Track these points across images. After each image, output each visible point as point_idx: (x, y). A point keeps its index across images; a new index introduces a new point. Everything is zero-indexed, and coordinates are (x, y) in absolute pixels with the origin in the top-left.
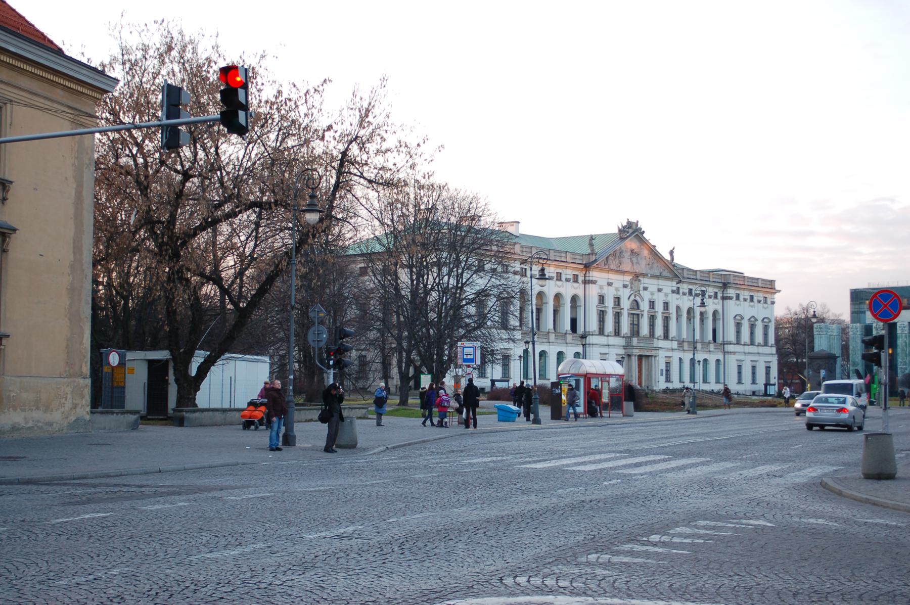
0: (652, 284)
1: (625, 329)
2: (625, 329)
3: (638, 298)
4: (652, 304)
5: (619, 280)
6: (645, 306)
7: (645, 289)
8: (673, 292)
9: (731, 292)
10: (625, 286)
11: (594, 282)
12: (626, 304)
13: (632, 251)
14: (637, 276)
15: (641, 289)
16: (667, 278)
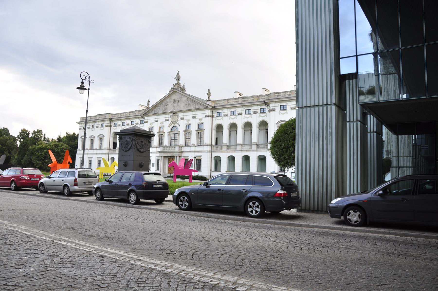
0: (188, 116)
1: (166, 142)
2: (166, 142)
3: (176, 125)
4: (188, 126)
5: (162, 118)
6: (182, 128)
7: (182, 119)
8: (207, 116)
9: (272, 106)
10: (167, 120)
11: (147, 122)
12: (167, 129)
13: (174, 100)
14: (175, 113)
15: (179, 119)
16: (197, 110)
